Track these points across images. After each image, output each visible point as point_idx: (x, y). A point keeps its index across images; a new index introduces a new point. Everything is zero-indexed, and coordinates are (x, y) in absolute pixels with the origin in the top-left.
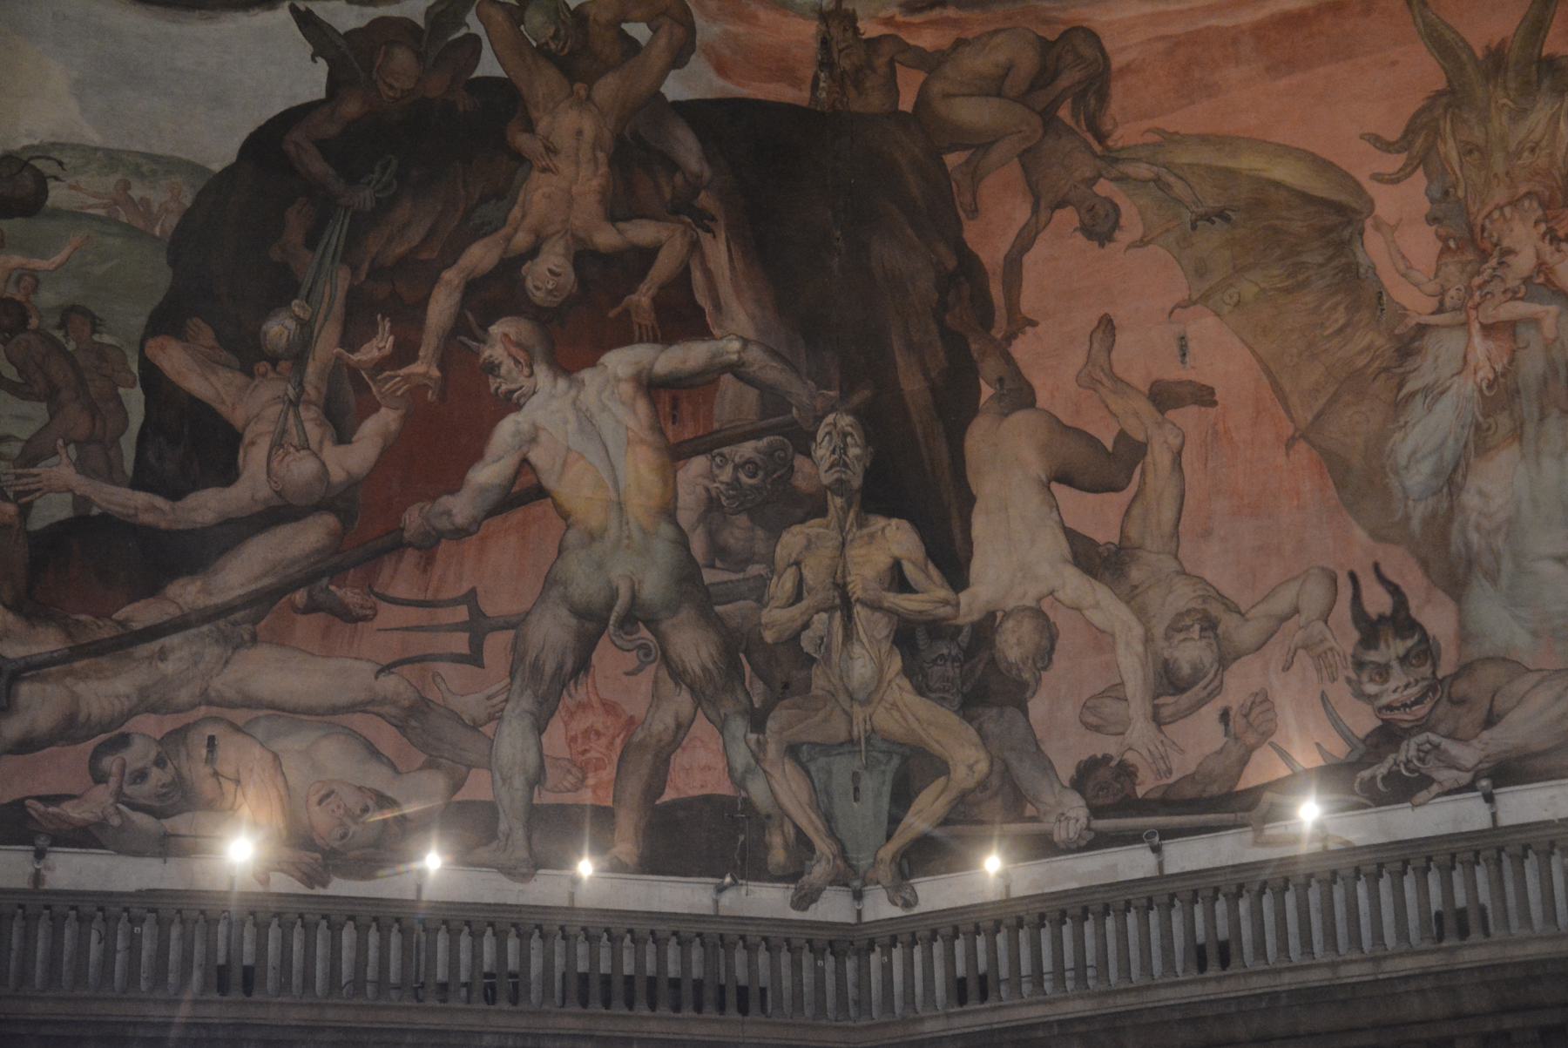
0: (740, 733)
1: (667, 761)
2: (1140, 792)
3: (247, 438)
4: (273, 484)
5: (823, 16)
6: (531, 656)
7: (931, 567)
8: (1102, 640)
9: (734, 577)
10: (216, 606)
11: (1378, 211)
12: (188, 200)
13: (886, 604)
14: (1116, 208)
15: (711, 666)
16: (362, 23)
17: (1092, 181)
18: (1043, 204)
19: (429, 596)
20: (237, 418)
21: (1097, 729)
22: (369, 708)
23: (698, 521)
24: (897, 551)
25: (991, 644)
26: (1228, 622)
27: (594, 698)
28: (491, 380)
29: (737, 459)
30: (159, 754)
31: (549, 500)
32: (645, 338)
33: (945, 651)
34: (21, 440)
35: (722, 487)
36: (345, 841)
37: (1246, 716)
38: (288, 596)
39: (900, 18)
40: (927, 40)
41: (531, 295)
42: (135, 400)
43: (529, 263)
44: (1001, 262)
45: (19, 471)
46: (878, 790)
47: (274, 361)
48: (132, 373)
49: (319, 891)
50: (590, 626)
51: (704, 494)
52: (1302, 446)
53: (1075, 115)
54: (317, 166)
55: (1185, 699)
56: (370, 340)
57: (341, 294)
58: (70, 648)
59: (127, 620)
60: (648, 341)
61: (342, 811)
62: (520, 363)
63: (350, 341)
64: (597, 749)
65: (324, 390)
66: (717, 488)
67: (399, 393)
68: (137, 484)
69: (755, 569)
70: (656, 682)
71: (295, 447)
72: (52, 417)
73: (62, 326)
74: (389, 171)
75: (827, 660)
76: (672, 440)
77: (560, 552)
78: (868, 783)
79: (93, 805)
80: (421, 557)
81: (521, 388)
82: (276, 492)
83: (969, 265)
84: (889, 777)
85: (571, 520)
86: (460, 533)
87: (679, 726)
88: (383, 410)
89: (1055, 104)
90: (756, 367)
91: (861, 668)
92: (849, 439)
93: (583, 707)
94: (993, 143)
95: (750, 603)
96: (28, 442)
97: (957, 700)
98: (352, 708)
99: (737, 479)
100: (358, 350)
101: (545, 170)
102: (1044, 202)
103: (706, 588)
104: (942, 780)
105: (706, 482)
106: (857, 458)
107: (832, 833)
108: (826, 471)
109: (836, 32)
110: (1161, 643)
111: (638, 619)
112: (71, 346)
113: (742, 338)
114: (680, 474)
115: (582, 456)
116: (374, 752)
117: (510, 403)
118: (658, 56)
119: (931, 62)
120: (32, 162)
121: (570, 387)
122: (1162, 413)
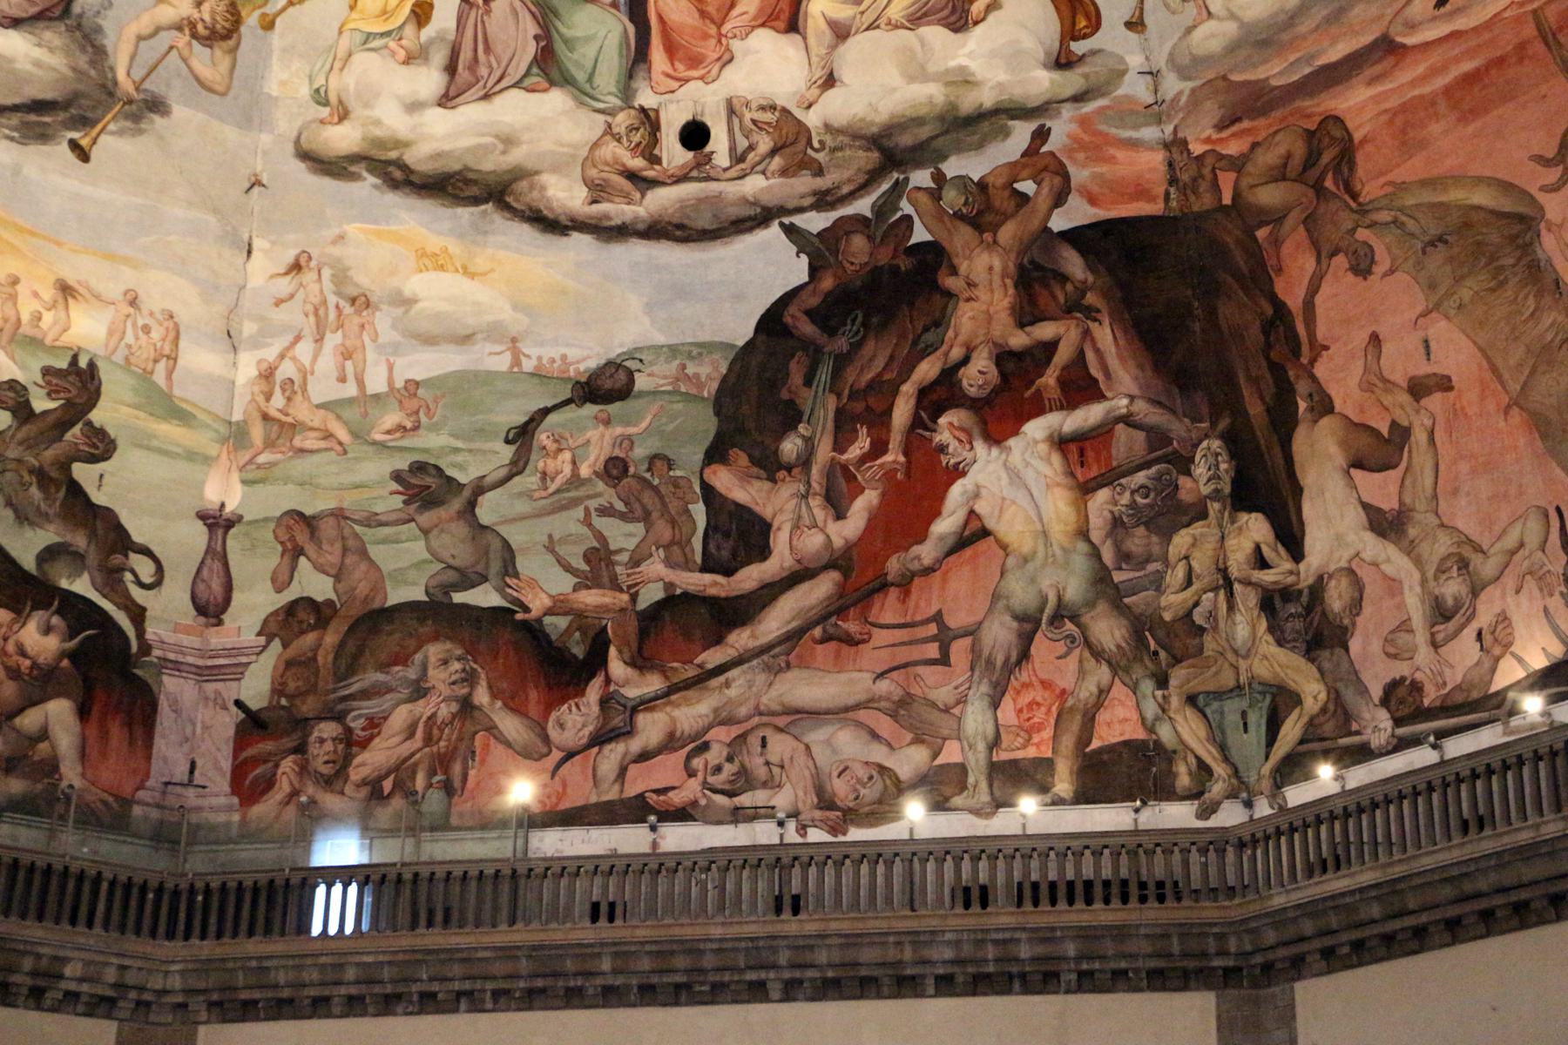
1: (1093, 718)
2: (1426, 702)
3: (775, 525)
5: (1167, 146)
6: (986, 653)
7: (1280, 547)
8: (1393, 586)
9: (1137, 574)
11: (1549, 216)
14: (1371, 247)
16: (828, 224)
17: (1354, 230)
18: (1324, 254)
19: (908, 619)
20: (767, 512)
21: (1395, 657)
23: (1107, 536)
24: (1258, 537)
25: (1322, 601)
26: (1476, 560)
37: (1493, 633)
39: (1215, 136)
40: (1233, 148)
42: (699, 511)
46: (1257, 719)
47: (789, 469)
49: (841, 838)
51: (1109, 516)
52: (1515, 411)
53: (1336, 184)
54: (807, 328)
55: (1451, 626)
57: (831, 415)
63: (840, 446)
64: (1039, 715)
68: (705, 568)
69: (1152, 567)
70: (1081, 661)
73: (649, 470)
75: (1215, 628)
76: (1081, 479)
77: (1002, 574)
78: (1253, 718)
79: (690, 790)
83: (1280, 308)
86: (928, 571)
87: (1101, 691)
89: (1321, 178)
91: (1242, 631)
93: (1026, 686)
94: (1285, 216)
95: (1150, 593)
97: (1304, 646)
98: (857, 707)
101: (968, 300)
102: (1323, 252)
104: (1296, 712)
105: (1111, 507)
106: (1227, 471)
107: (1226, 759)
109: (1176, 156)
110: (1432, 584)
111: (1063, 617)
112: (656, 482)
115: (1014, 502)
116: (875, 736)
117: (958, 472)
118: (1043, 203)
119: (1238, 164)
122: (1418, 401)
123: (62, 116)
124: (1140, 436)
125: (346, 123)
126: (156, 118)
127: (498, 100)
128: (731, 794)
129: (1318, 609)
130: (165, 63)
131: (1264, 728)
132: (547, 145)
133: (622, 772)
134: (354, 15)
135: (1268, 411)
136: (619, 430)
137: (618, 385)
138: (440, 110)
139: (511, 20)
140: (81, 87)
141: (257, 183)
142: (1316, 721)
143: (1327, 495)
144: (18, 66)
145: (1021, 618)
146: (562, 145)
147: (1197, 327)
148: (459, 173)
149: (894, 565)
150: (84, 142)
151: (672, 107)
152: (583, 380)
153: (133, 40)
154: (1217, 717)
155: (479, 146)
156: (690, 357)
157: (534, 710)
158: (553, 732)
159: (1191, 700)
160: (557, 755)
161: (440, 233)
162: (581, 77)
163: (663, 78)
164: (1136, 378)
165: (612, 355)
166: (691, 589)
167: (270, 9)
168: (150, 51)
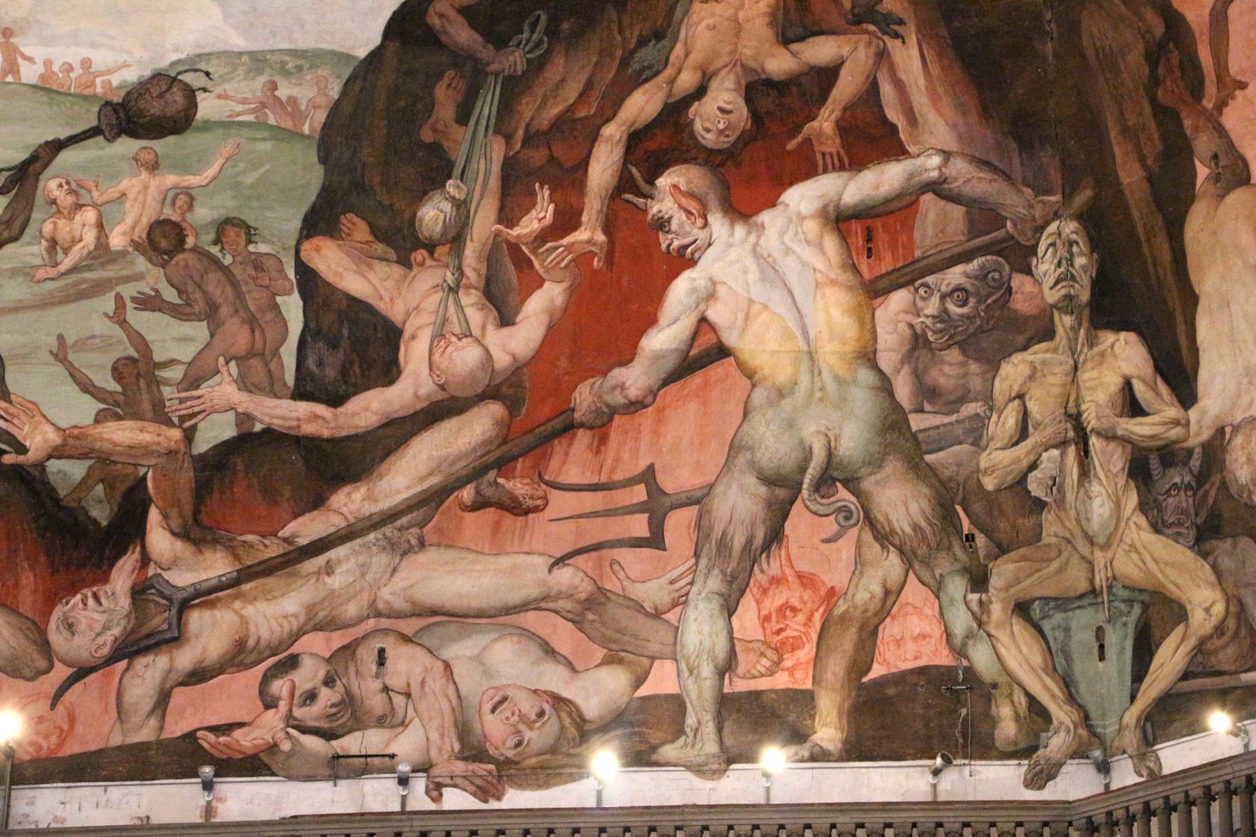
0: (959, 596)
1: (874, 633)
4: (436, 378)
7: (1159, 381)
9: (946, 420)
10: (382, 512)
12: (335, 92)
13: (1120, 433)
15: (923, 524)
19: (604, 479)
20: (396, 312)
22: (543, 605)
23: (903, 362)
24: (1128, 369)
25: (1222, 467)
27: (788, 571)
28: (661, 236)
29: (943, 288)
30: (328, 672)
31: (732, 359)
32: (830, 167)
33: (1178, 480)
34: (183, 363)
35: (928, 322)
36: (520, 749)
38: (456, 494)
41: (700, 139)
42: (293, 307)
43: (696, 104)
44: (1207, 19)
45: (183, 395)
46: (1120, 641)
47: (431, 247)
48: (289, 280)
49: (494, 805)
50: (782, 493)
51: (907, 332)
54: (462, 35)
56: (528, 211)
57: (496, 169)
58: (238, 571)
59: (294, 536)
60: (834, 169)
61: (516, 718)
62: (692, 214)
63: (508, 215)
64: (795, 626)
65: (484, 272)
66: (922, 322)
67: (563, 265)
68: (300, 394)
69: (969, 409)
70: (859, 547)
71: (456, 335)
72: (212, 336)
73: (217, 241)
74: (538, 29)
75: (1061, 503)
76: (867, 276)
77: (746, 414)
79: (269, 726)
80: (594, 437)
81: (695, 242)
82: (438, 385)
84: (1131, 629)
85: (756, 378)
86: (636, 406)
87: (887, 593)
88: (547, 285)
90: (959, 183)
91: (1100, 509)
92: (1075, 249)
93: (776, 581)
95: (965, 448)
96: (190, 364)
97: (1193, 532)
98: (524, 607)
99: (946, 311)
100: (517, 224)
103: (914, 436)
104: (1180, 629)
106: (1084, 268)
107: (1071, 698)
108: (1051, 288)
111: (834, 480)
112: (227, 261)
113: (944, 152)
114: (878, 313)
115: (765, 307)
116: (550, 652)
117: (683, 260)
120: (180, 77)
121: (749, 233)
124: (957, 213)
128: (328, 735)
129: (1216, 478)
131: (1129, 653)
133: (163, 700)
135: (1151, 179)
136: (171, 179)
137: (170, 111)
142: (1209, 646)
143: (1234, 307)
145: (769, 480)
147: (1048, 49)
149: (584, 397)
152: (117, 99)
154: (1060, 635)
156: (285, 73)
157: (27, 600)
158: (57, 637)
159: (1022, 609)
160: (61, 672)
164: (955, 126)
165: (163, 63)
166: (277, 423)
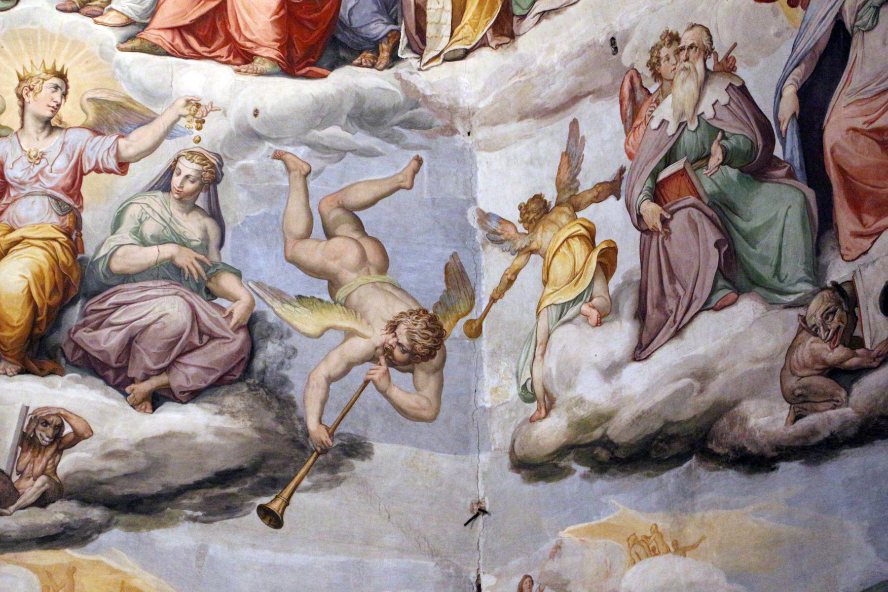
123: (249, 483)
125: (553, 413)
126: (359, 465)
127: (689, 333)
130: (360, 400)
132: (742, 367)
134: (549, 290)
138: (636, 365)
139: (691, 236)
140: (268, 447)
141: (482, 511)
144: (199, 440)
146: (757, 361)
148: (660, 432)
150: (275, 507)
151: (868, 272)
153: (322, 381)
155: (677, 392)
161: (650, 510)
162: (766, 272)
163: (852, 239)
167: (474, 315)
168: (341, 393)
